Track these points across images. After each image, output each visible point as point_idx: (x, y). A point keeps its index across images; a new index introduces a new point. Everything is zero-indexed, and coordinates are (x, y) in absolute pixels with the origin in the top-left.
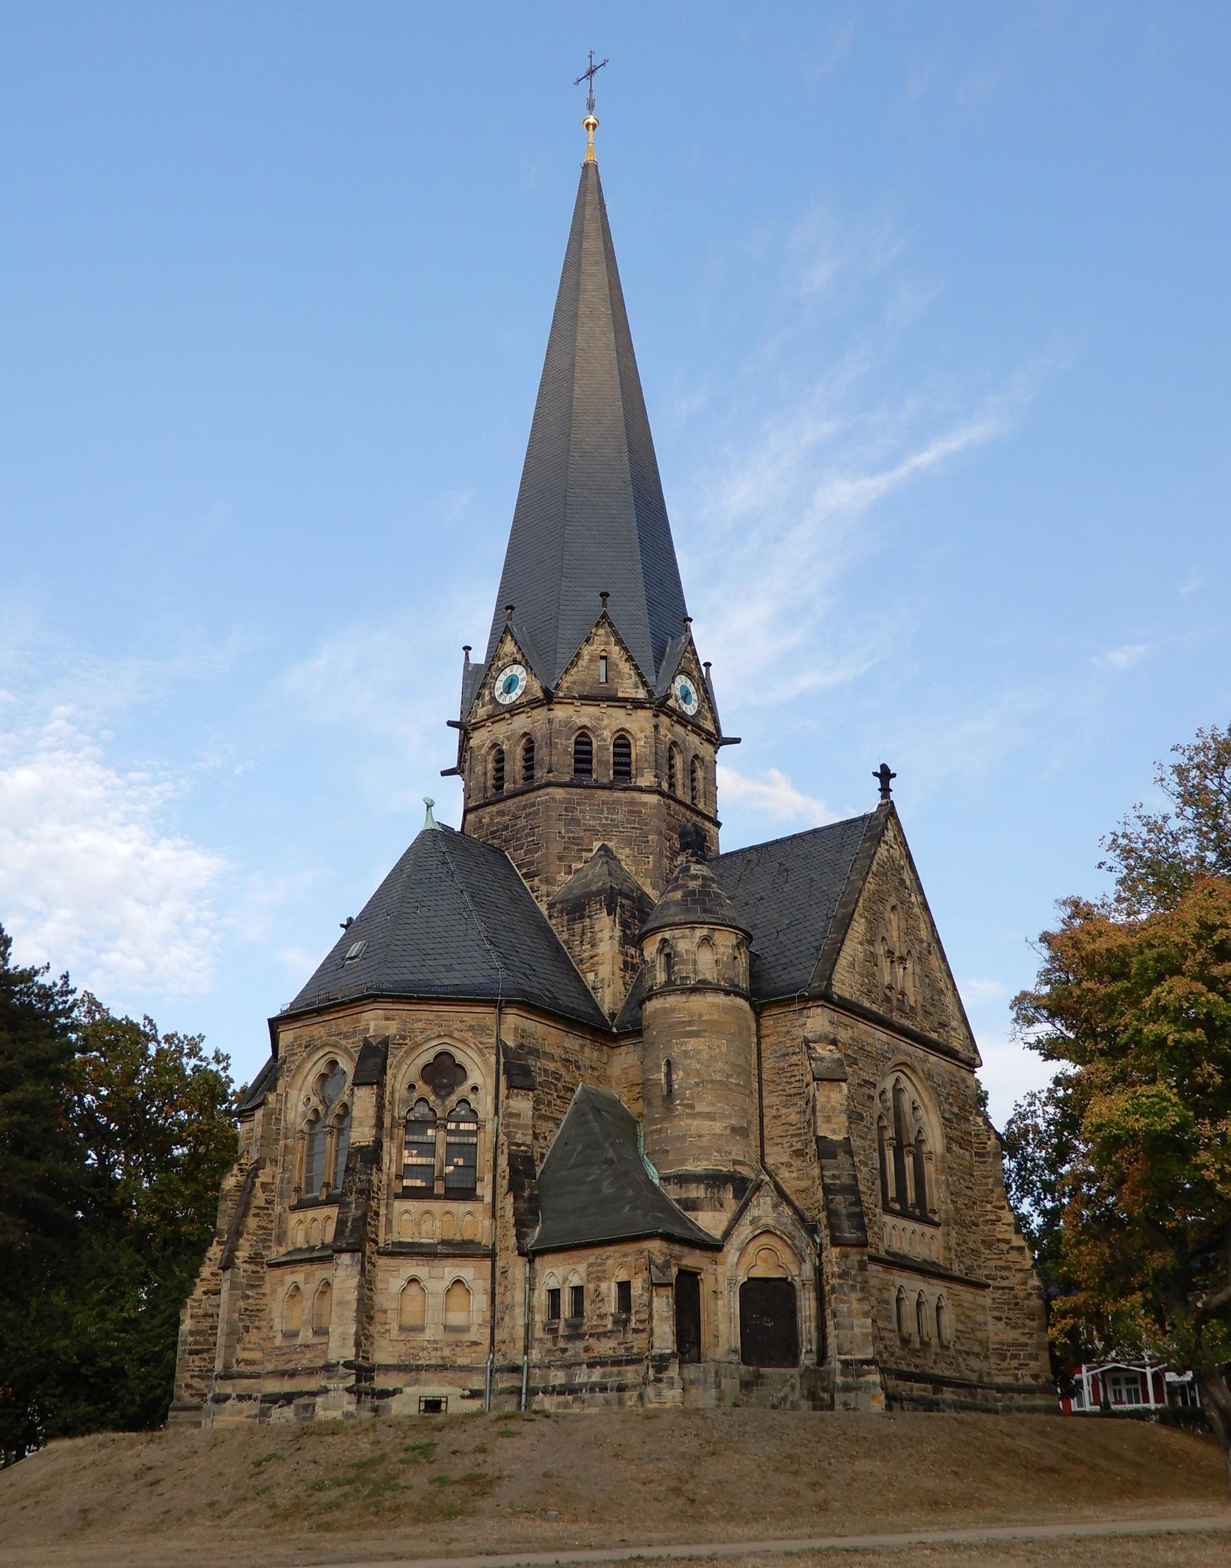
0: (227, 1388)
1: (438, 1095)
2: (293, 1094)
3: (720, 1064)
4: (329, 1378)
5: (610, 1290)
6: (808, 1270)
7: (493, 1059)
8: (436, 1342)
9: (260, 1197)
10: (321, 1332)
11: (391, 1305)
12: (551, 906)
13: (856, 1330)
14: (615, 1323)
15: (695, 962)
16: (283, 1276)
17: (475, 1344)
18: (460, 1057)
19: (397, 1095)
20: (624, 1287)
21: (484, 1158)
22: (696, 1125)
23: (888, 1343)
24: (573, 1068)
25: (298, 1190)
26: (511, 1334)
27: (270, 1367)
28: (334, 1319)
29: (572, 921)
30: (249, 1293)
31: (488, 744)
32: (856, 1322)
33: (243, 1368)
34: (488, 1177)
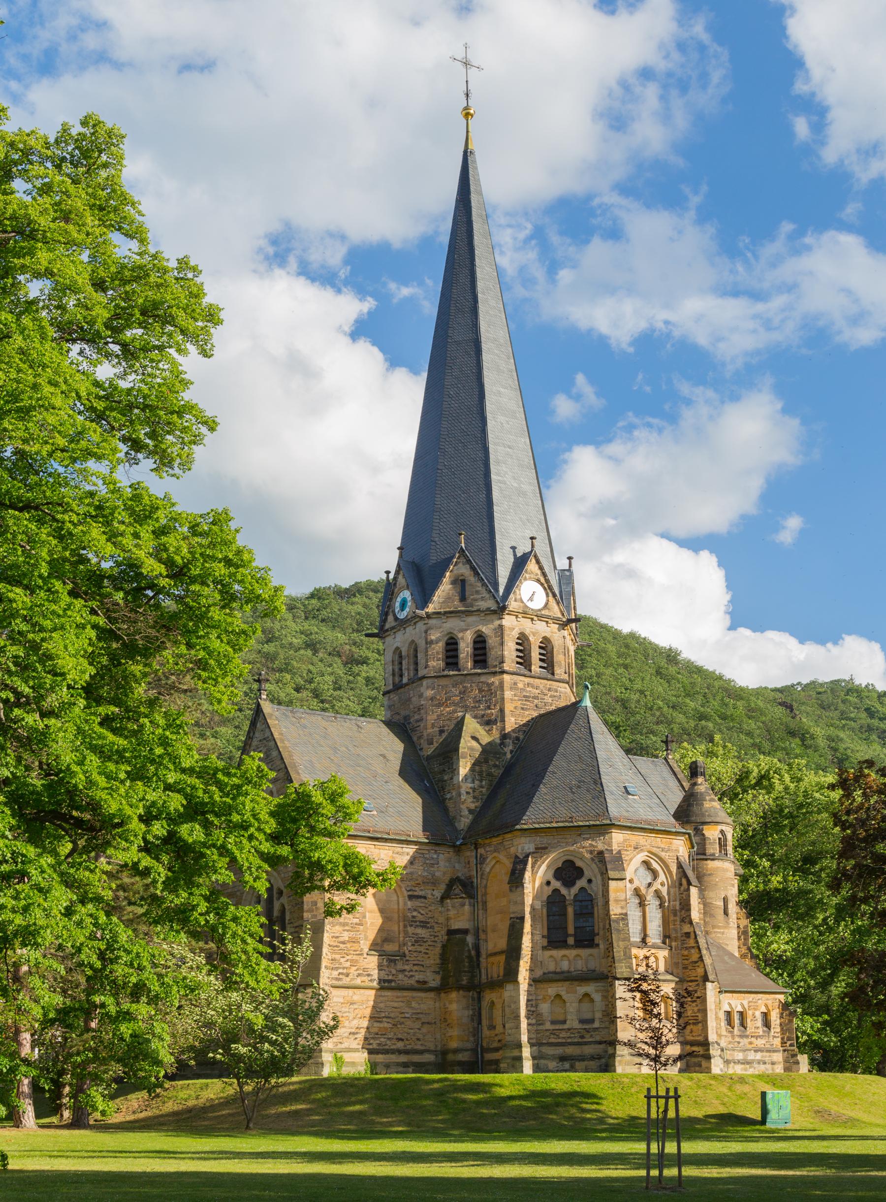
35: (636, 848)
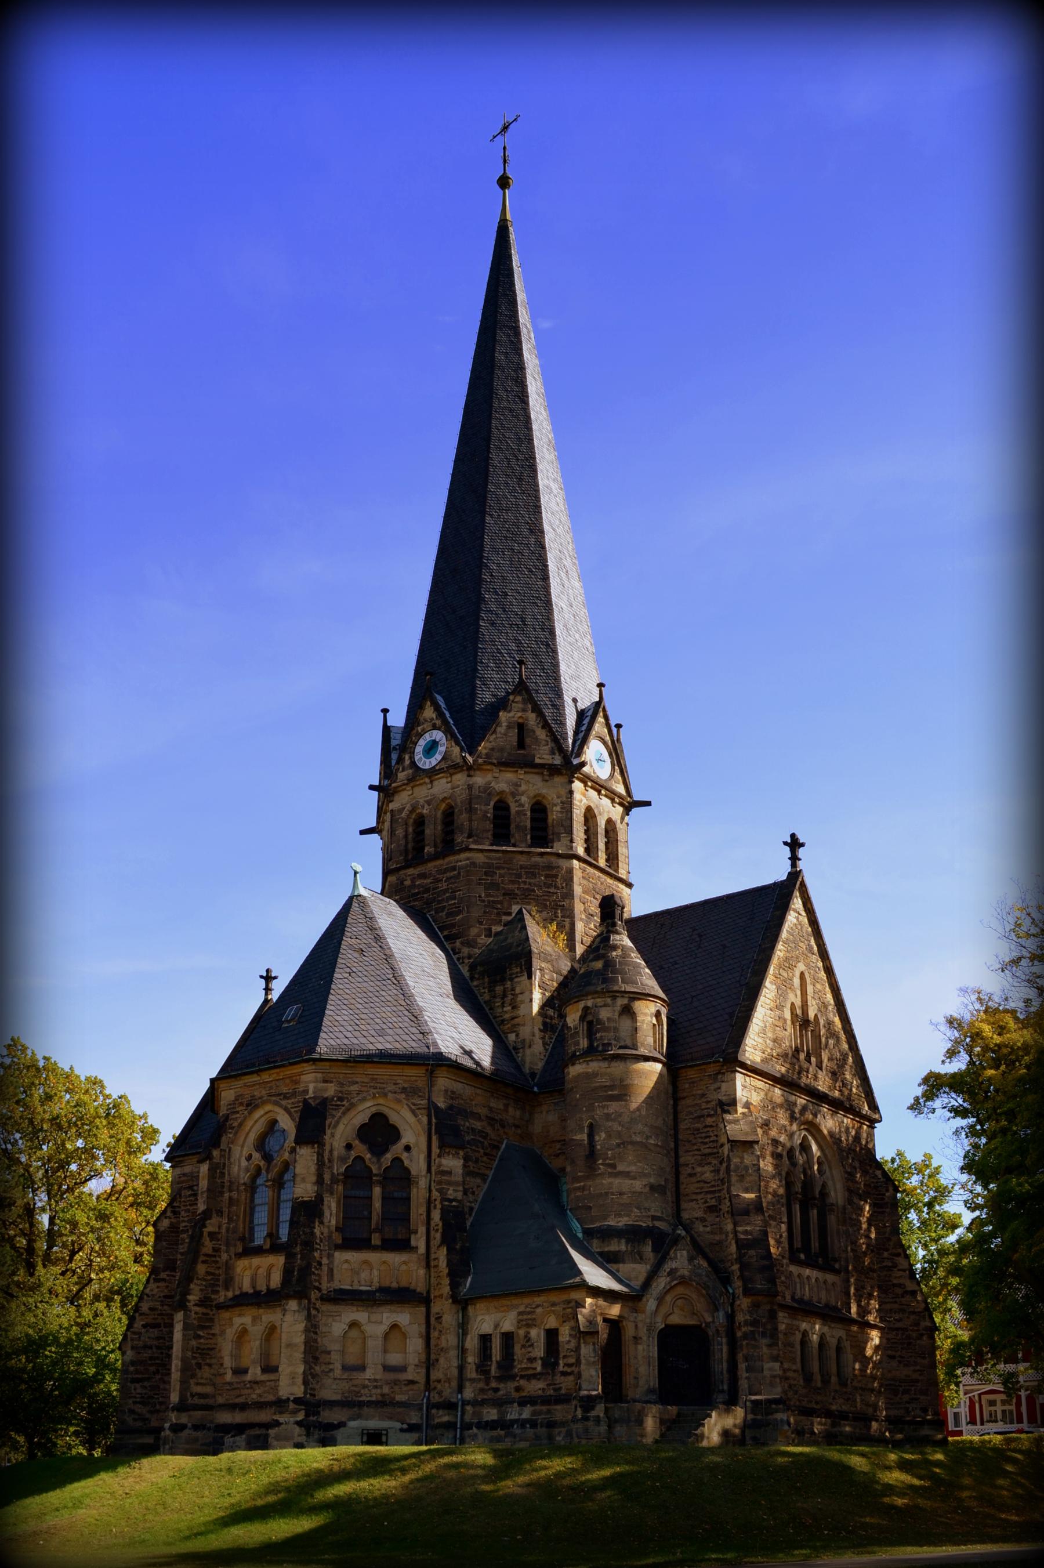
0: (184, 1419)
1: (373, 1153)
2: (236, 1150)
3: (640, 1127)
4: (281, 1413)
5: (537, 1334)
6: (721, 1317)
7: (425, 1119)
8: (376, 1380)
9: (208, 1246)
10: (270, 1369)
11: (335, 1347)
12: (472, 968)
13: (766, 1373)
14: (544, 1365)
15: (616, 1029)
16: (231, 1319)
17: (412, 1382)
18: (394, 1119)
19: (336, 1154)
20: (552, 1335)
21: (417, 1211)
22: (617, 1183)
23: (792, 1382)
24: (497, 1126)
25: (242, 1239)
26: (446, 1375)
27: (221, 1400)
28: (283, 1360)
29: (493, 983)
30: (201, 1333)
31: (408, 807)
32: (766, 1366)
33: (197, 1401)
34: (422, 1230)
35: (248, 1105)
